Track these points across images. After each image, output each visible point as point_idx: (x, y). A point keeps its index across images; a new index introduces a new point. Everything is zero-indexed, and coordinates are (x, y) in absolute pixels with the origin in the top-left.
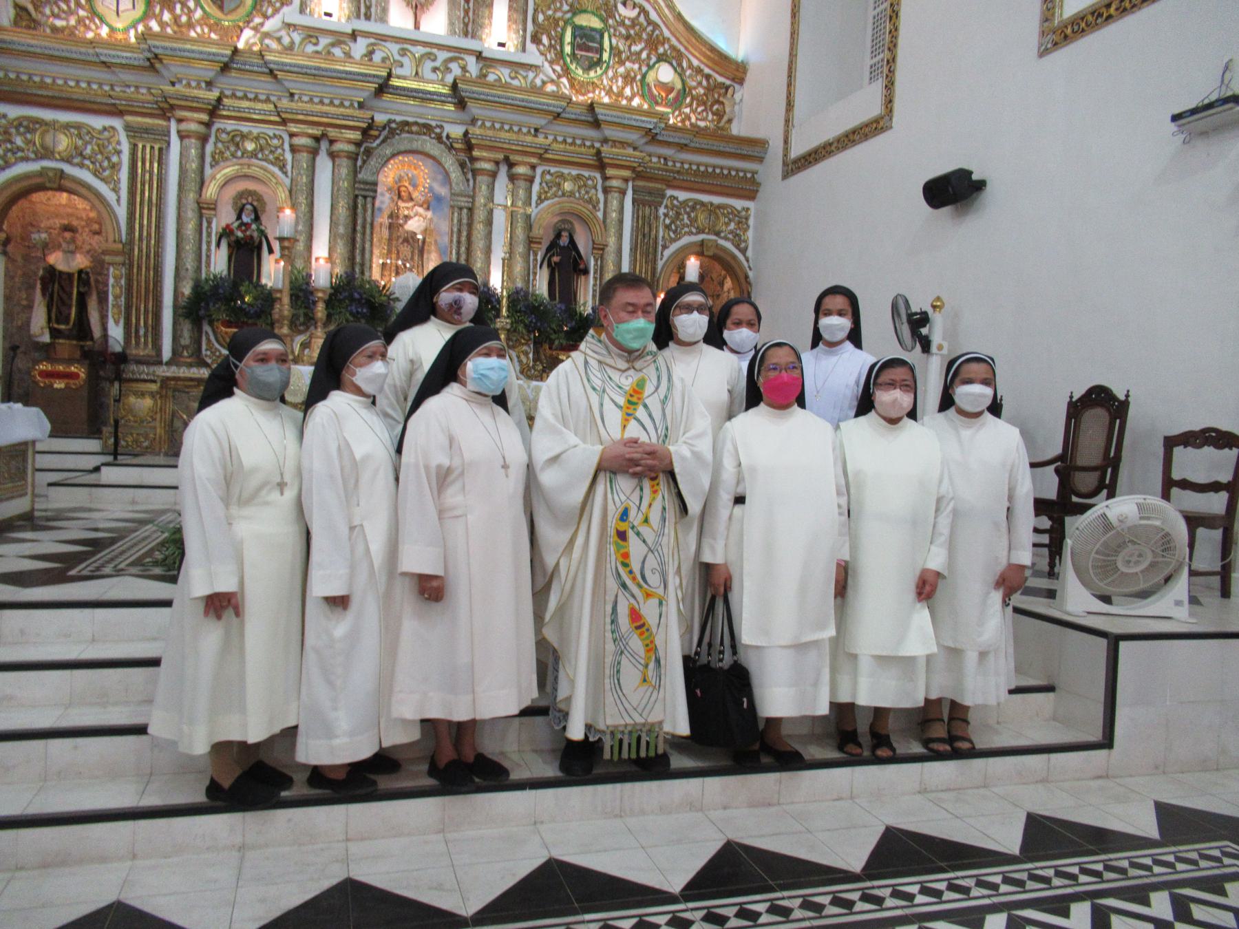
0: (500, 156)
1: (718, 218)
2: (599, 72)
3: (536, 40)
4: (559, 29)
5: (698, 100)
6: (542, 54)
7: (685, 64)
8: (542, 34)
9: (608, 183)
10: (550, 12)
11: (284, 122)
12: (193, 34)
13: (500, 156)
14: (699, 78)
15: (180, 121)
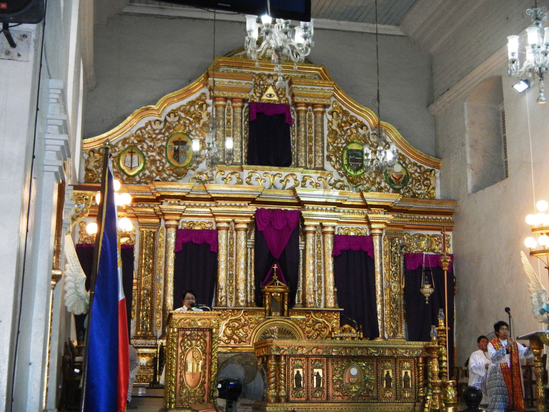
0: (318, 223)
1: (432, 242)
2: (362, 171)
3: (329, 159)
4: (340, 152)
5: (416, 179)
6: (334, 166)
7: (407, 162)
8: (332, 156)
9: (373, 231)
10: (335, 145)
11: (214, 216)
12: (165, 175)
13: (318, 223)
14: (416, 168)
15: (166, 220)
